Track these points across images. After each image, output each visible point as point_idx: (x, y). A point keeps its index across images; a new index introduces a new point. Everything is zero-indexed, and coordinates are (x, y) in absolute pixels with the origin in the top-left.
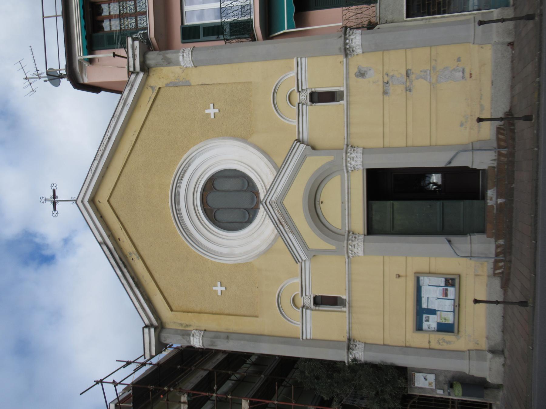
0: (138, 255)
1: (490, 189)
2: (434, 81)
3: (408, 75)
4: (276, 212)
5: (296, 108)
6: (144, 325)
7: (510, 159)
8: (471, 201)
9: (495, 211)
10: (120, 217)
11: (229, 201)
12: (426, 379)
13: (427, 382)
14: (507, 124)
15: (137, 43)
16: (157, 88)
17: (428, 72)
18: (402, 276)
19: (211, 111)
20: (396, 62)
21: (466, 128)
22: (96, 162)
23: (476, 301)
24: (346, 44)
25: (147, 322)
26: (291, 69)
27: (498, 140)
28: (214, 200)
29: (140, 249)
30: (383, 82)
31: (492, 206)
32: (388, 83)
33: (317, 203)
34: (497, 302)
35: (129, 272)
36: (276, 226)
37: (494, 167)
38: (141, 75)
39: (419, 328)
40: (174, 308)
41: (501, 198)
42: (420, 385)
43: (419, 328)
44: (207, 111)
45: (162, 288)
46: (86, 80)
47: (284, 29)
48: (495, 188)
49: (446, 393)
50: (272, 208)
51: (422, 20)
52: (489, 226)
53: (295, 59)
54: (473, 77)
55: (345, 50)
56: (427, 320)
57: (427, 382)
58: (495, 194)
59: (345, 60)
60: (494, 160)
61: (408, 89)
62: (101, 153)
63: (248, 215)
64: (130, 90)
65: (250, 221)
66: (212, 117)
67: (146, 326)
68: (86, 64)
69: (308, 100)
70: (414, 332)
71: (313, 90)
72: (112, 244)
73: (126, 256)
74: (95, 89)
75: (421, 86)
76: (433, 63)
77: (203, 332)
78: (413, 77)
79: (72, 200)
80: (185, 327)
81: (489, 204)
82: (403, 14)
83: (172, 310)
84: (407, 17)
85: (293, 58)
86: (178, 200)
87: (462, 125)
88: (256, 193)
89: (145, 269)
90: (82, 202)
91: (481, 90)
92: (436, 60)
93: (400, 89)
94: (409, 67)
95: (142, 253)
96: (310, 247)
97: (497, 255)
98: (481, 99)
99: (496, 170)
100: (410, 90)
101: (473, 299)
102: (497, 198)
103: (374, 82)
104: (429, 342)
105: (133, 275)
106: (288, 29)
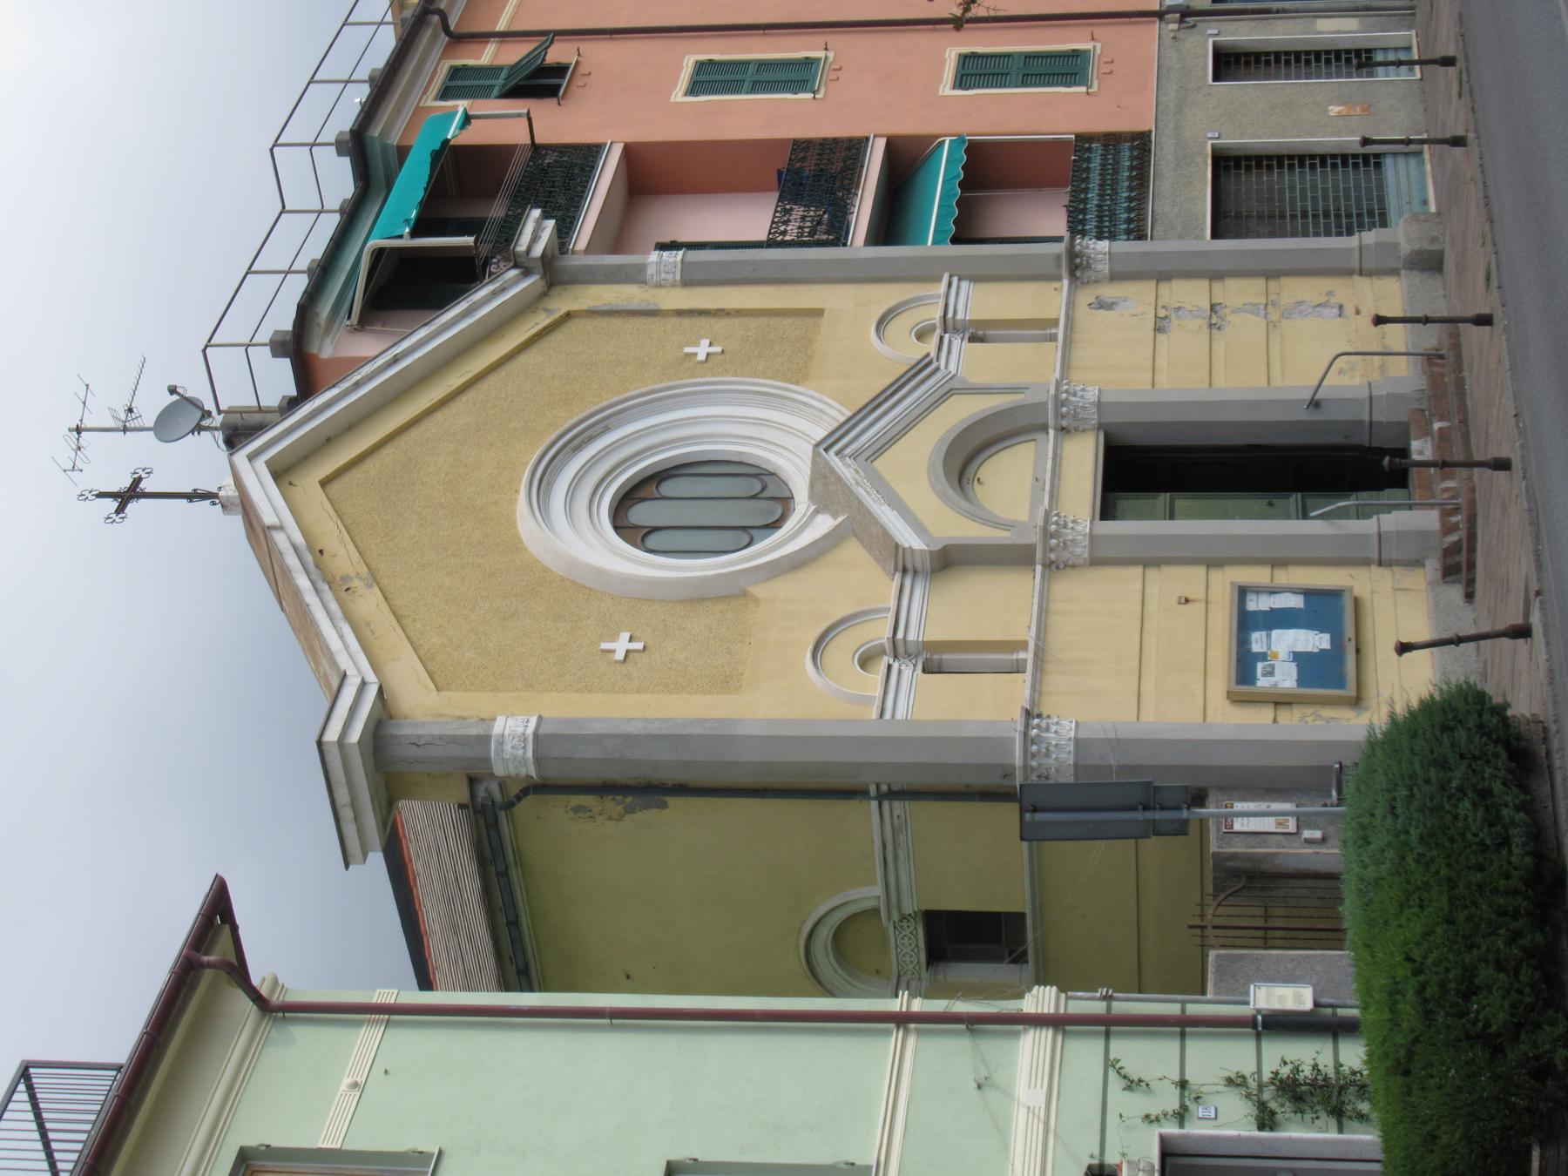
23: (1403, 648)
38: (532, 279)
53: (946, 276)
64: (495, 294)
76: (1272, 297)
85: (939, 280)
101: (1392, 646)
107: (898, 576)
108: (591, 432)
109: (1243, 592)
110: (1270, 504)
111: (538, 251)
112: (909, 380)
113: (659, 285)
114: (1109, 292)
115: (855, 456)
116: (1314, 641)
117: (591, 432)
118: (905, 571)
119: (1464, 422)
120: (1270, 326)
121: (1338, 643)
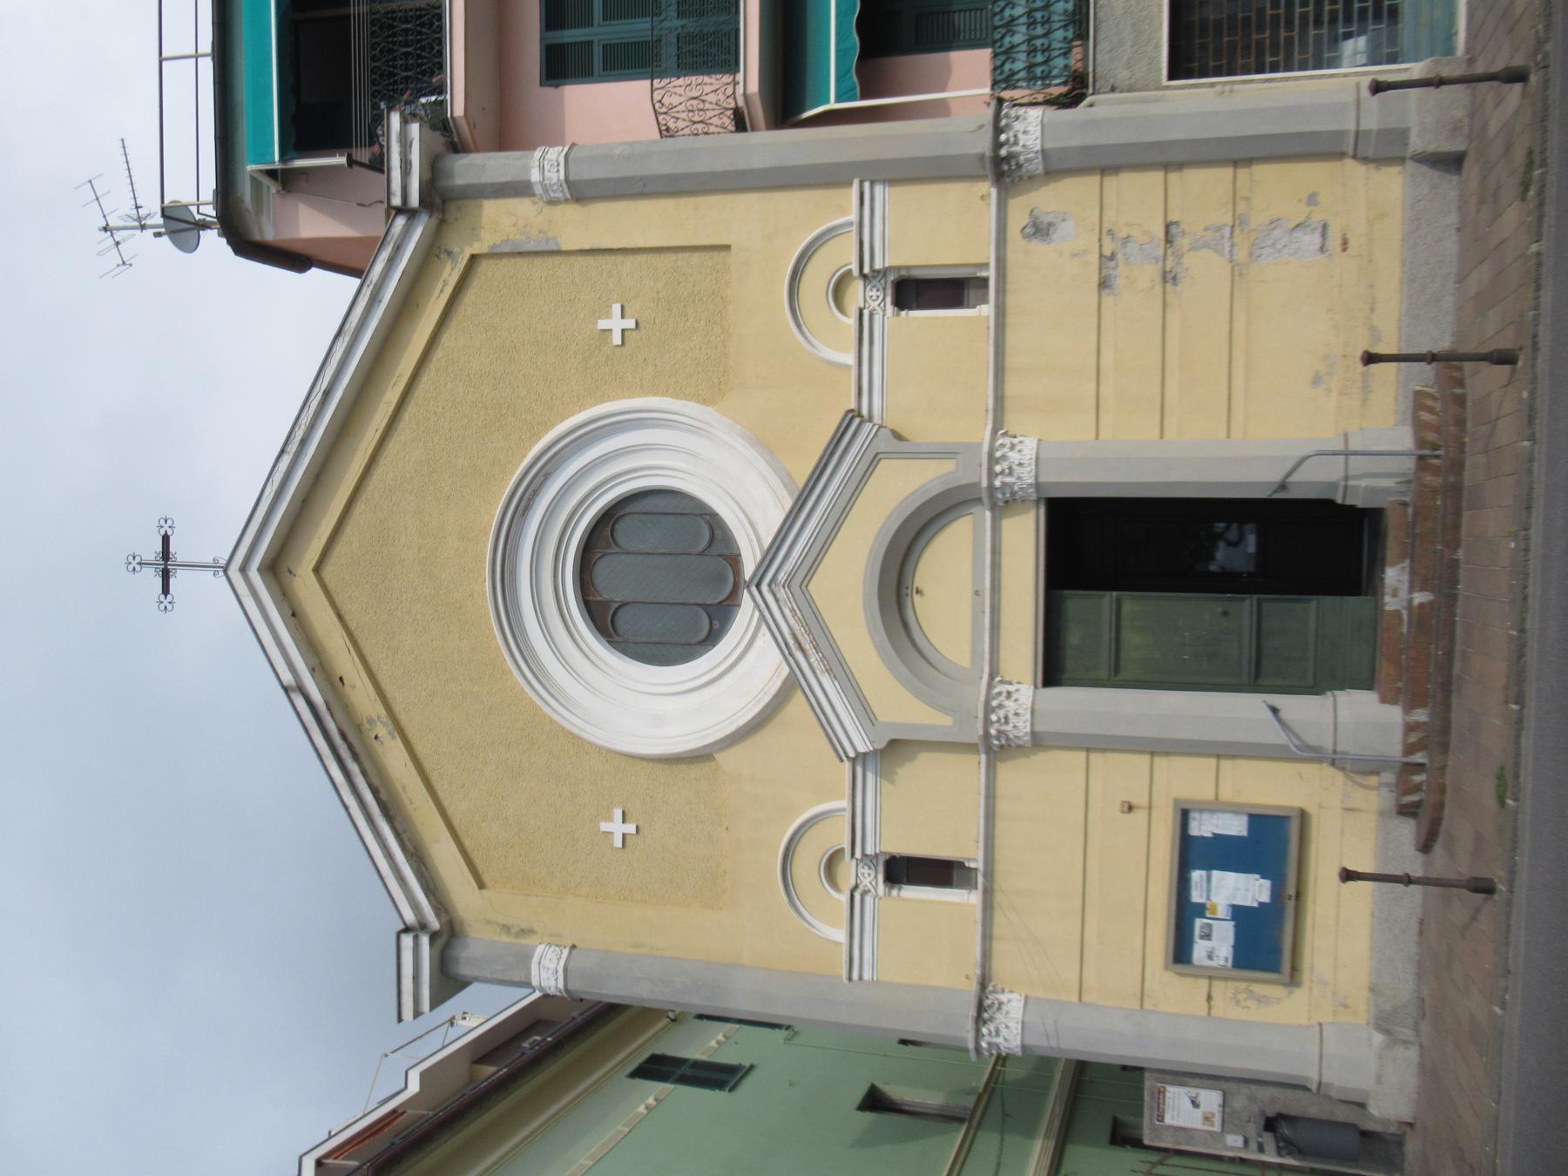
0: (391, 727)
1: (1393, 565)
2: (1241, 255)
3: (1168, 240)
4: (787, 612)
5: (852, 321)
6: (402, 927)
7: (1452, 479)
8: (1338, 598)
9: (1404, 630)
10: (347, 618)
11: (655, 576)
12: (1195, 1104)
13: (1198, 1113)
14: (1449, 377)
15: (415, 128)
16: (466, 256)
17: (1227, 231)
18: (1138, 807)
19: (615, 324)
20: (1137, 200)
21: (1329, 390)
22: (286, 459)
24: (998, 145)
25: (410, 917)
26: (843, 210)
27: (1419, 426)
28: (613, 580)
29: (398, 708)
30: (1101, 255)
31: (1398, 612)
32: (1112, 257)
33: (904, 591)
34: (1407, 880)
35: (364, 773)
36: (787, 655)
37: (1405, 504)
39: (1181, 952)
40: (486, 878)
41: (1422, 589)
42: (1181, 1123)
43: (1181, 952)
44: (603, 324)
45: (456, 823)
46: (269, 233)
47: (828, 101)
48: (1407, 563)
49: (1253, 1146)
50: (777, 600)
51: (1213, 85)
52: (1385, 669)
53: (856, 183)
54: (1352, 245)
55: (998, 161)
56: (1207, 936)
57: (1198, 1114)
58: (1406, 577)
59: (994, 192)
60: (1409, 482)
61: (1169, 278)
62: (299, 434)
63: (707, 621)
64: (391, 261)
65: (712, 638)
66: (617, 340)
67: (407, 929)
68: (272, 188)
69: (889, 299)
70: (1166, 968)
71: (904, 273)
72: (321, 691)
73: (358, 728)
74: (294, 258)
75: (1205, 270)
77: (566, 952)
78: (1182, 242)
79: (213, 566)
80: (517, 935)
81: (1387, 608)
82: (1160, 70)
83: (481, 885)
84: (1171, 77)
85: (850, 184)
86: (514, 573)
87: (1316, 380)
88: (734, 561)
89: (411, 765)
90: (243, 569)
91: (1372, 286)
92: (1247, 199)
93: (1147, 274)
94: (1172, 217)
95: (404, 720)
96: (884, 716)
97: (1409, 749)
98: (1372, 310)
99: (1410, 510)
100: (1174, 278)
102: (1411, 590)
103: (1075, 255)
104: (1209, 998)
105: (376, 782)
106: (838, 100)
107: (847, 765)
108: (534, 486)
109: (1185, 816)
110: (1225, 613)
111: (414, 200)
112: (832, 453)
113: (552, 202)
114: (1046, 199)
115: (788, 584)
116: (1251, 889)
117: (534, 486)
118: (853, 761)
119: (1453, 598)
120: (1237, 272)
121: (1277, 892)
